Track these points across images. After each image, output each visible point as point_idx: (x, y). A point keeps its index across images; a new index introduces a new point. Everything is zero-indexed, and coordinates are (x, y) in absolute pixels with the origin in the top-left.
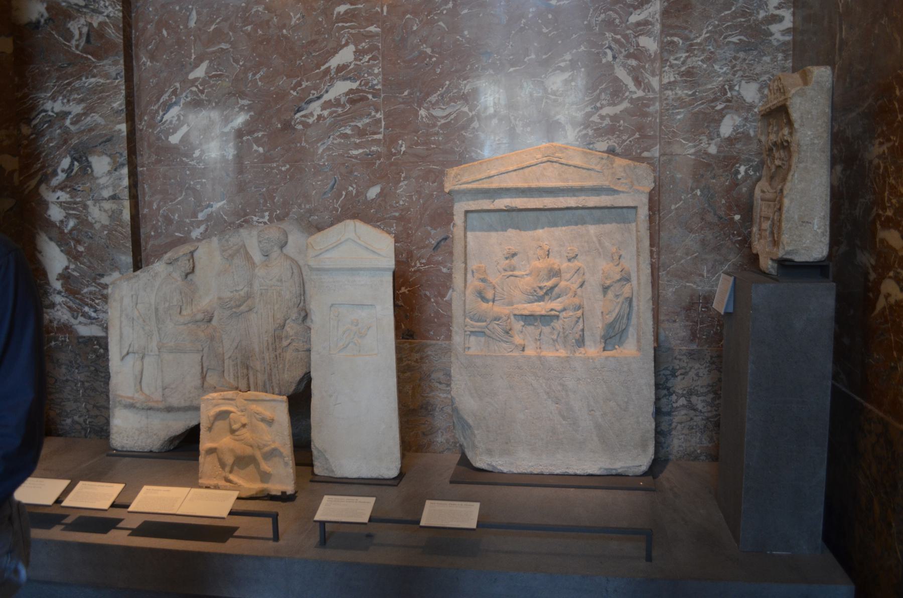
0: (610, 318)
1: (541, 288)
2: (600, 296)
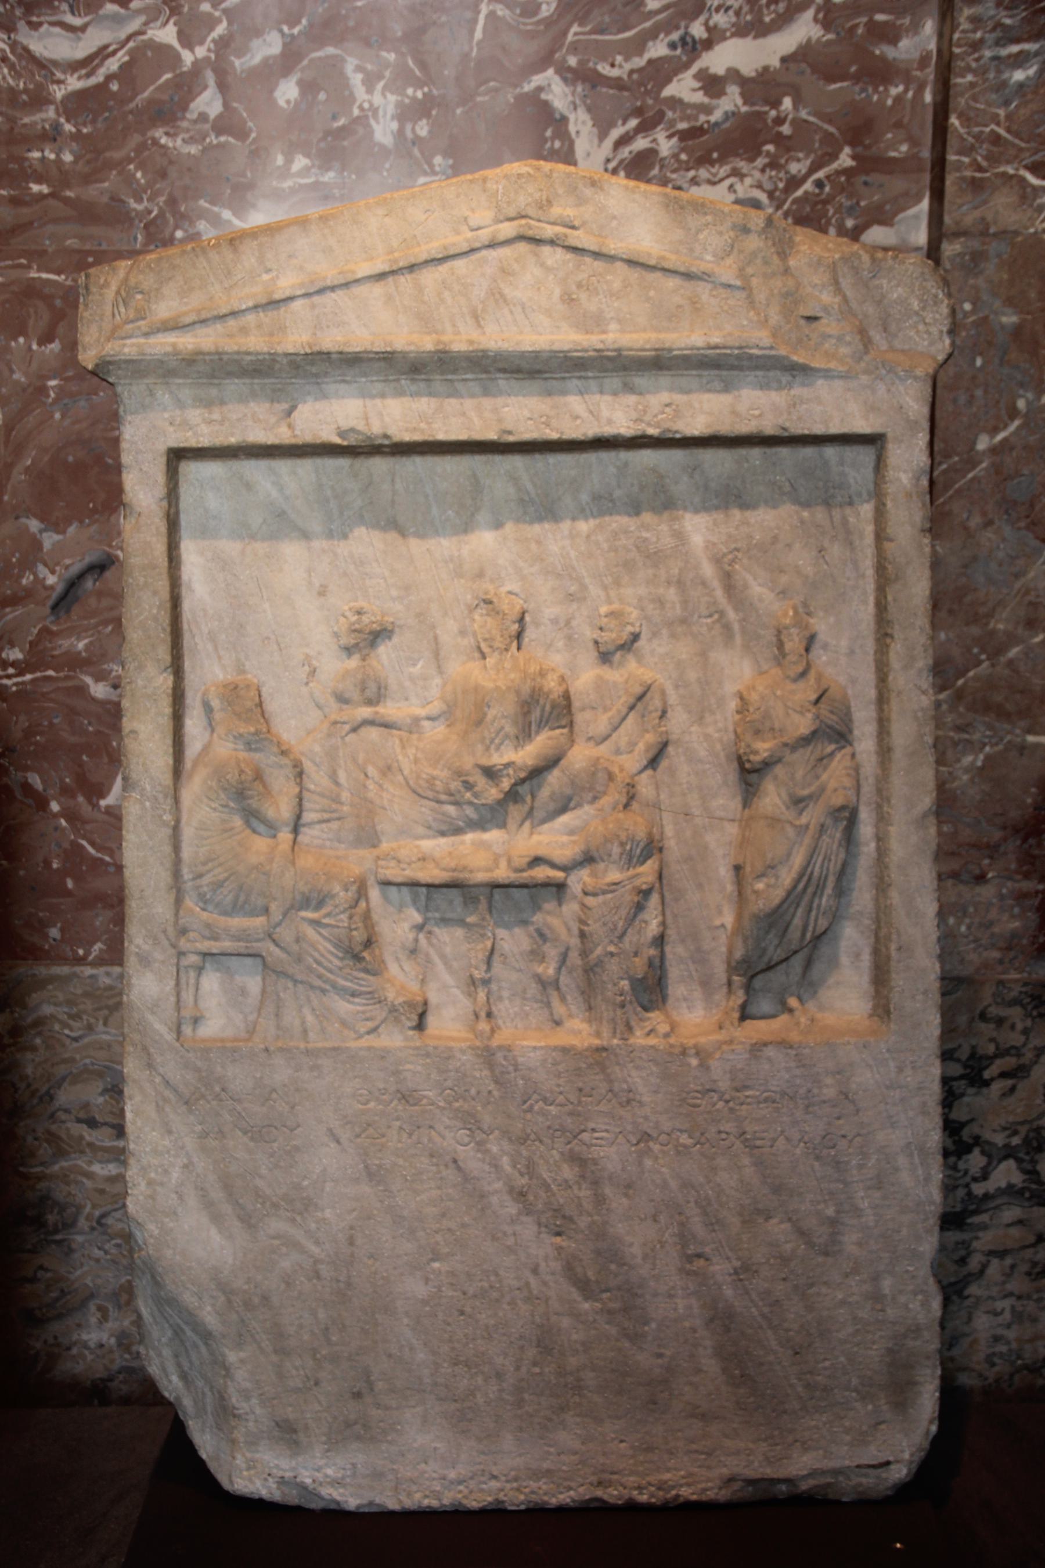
0: (768, 892)
1: (490, 773)
2: (727, 802)
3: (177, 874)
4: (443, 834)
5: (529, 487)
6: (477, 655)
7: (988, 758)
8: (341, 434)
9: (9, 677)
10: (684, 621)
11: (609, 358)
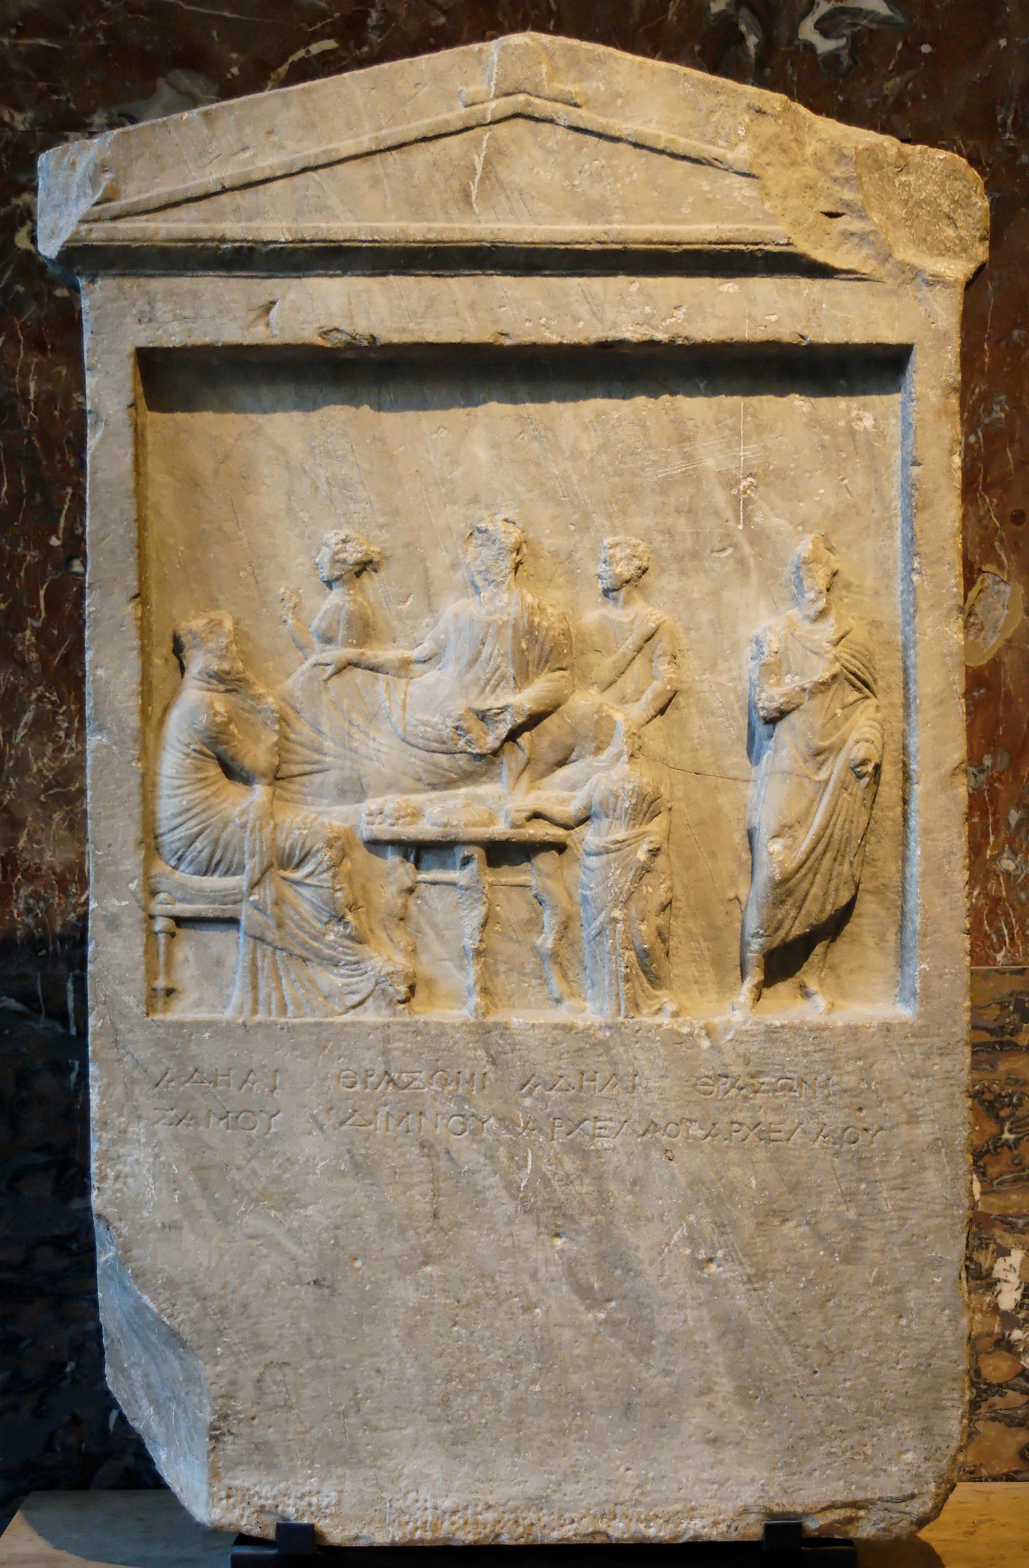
1: (483, 716)
6: (471, 590)
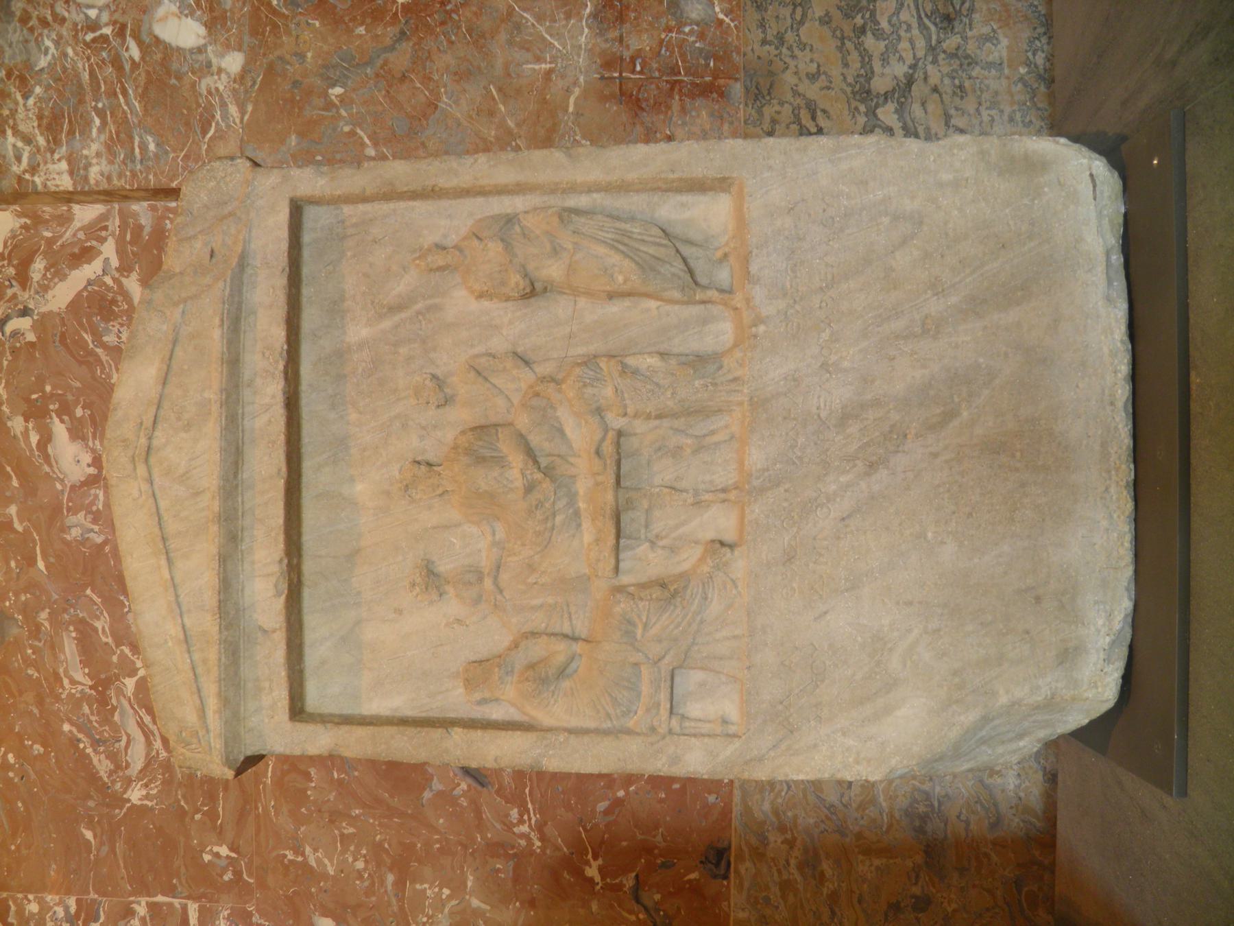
0: (624, 272)
1: (529, 488)
2: (561, 307)
3: (606, 733)
4: (579, 525)
5: (325, 456)
6: (446, 497)
7: (584, 137)
8: (278, 594)
9: (530, 819)
10: (424, 342)
11: (227, 398)
